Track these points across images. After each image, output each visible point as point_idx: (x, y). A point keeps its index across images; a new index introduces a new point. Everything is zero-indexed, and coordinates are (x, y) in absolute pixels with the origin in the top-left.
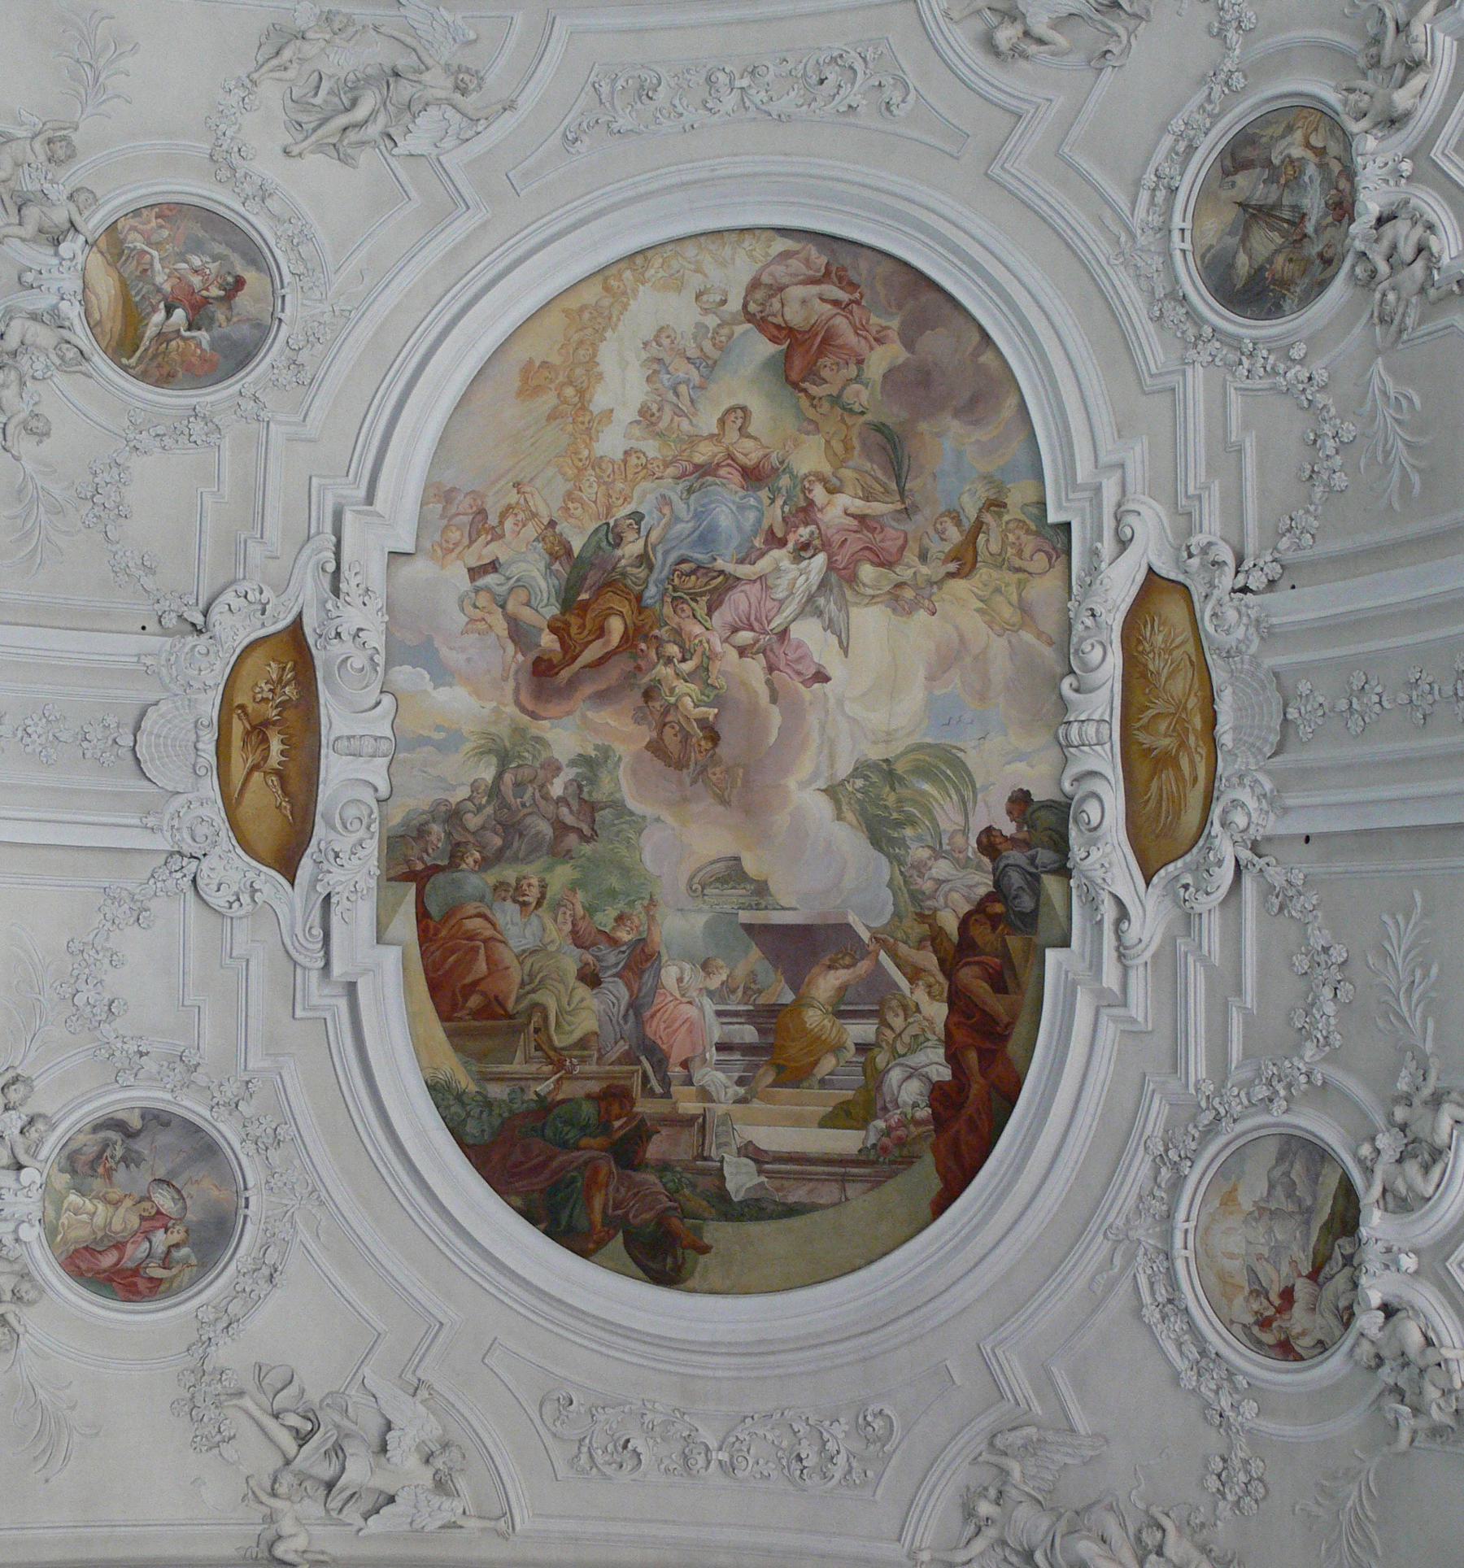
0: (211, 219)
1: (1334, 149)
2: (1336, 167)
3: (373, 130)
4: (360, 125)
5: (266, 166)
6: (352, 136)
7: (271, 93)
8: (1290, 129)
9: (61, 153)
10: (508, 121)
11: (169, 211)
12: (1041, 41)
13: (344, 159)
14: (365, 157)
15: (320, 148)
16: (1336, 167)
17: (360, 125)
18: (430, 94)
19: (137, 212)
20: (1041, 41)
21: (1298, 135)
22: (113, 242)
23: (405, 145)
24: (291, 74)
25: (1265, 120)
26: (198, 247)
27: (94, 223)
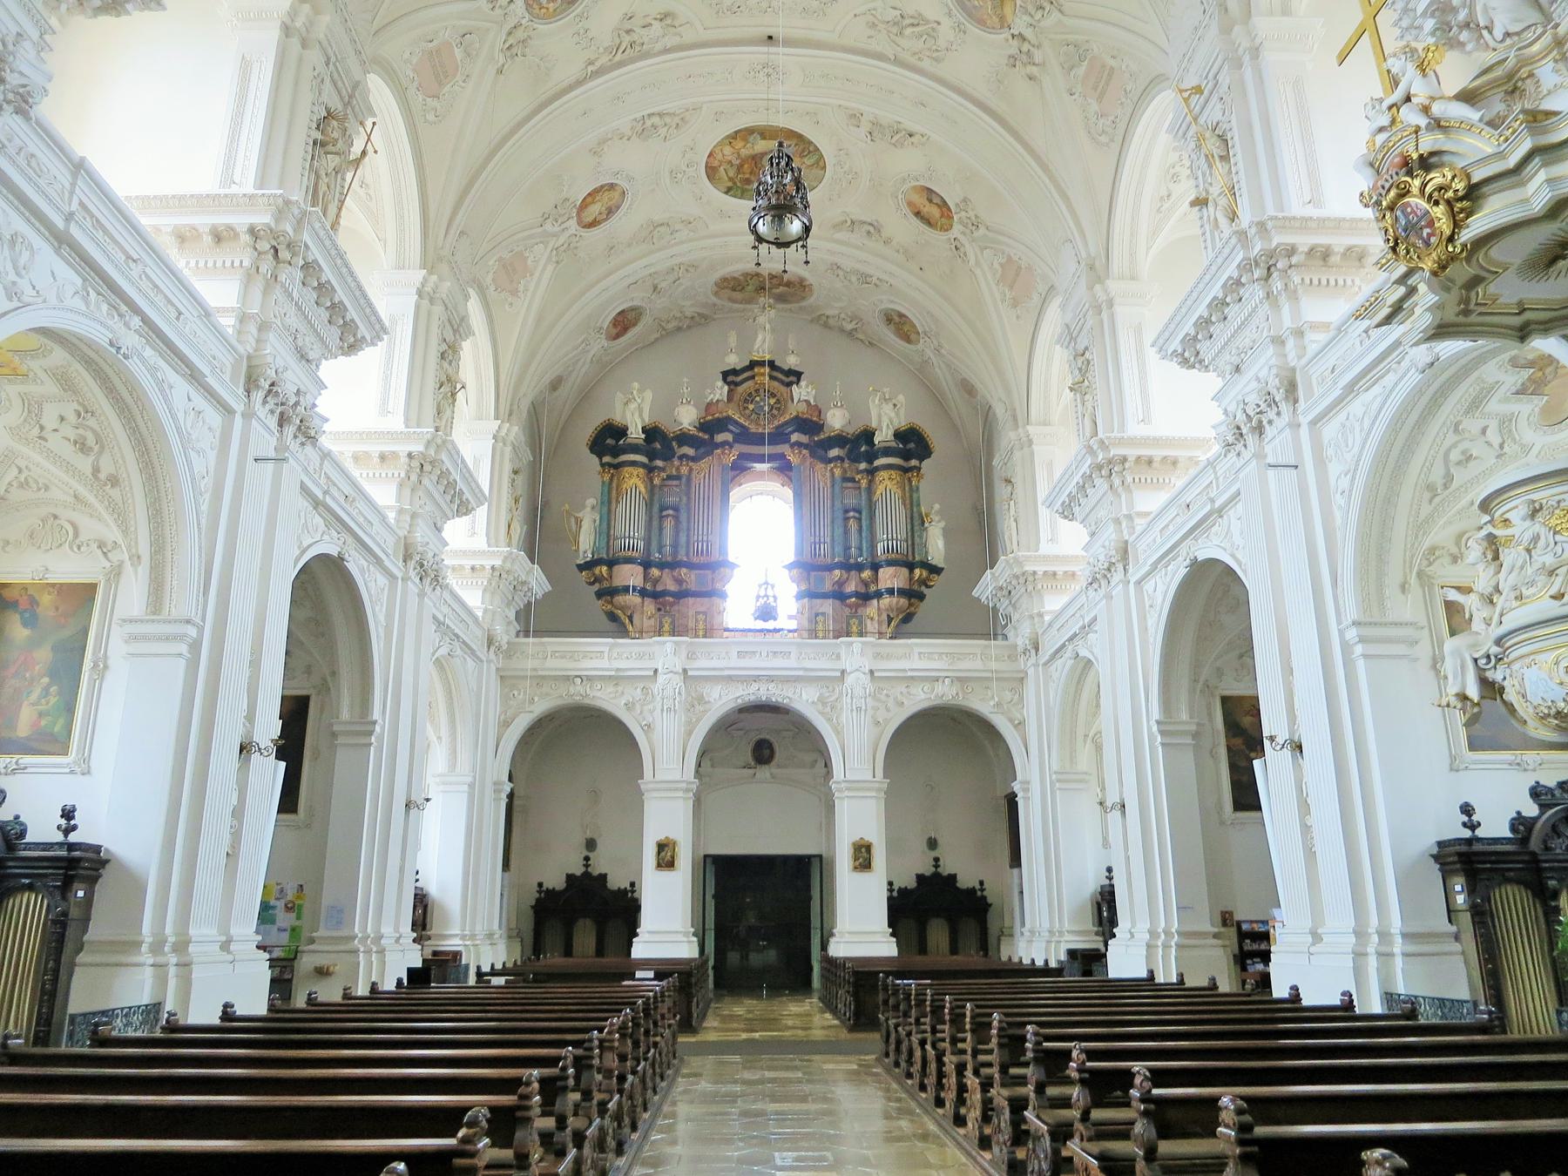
0: (970, 15)
1: (537, 11)
2: (535, 6)
3: (908, 21)
4: (913, 25)
5: (947, 23)
6: (916, 22)
7: (942, 43)
8: (555, 10)
9: (1012, 60)
10: (857, 12)
11: (981, 23)
12: (656, 19)
13: (920, 15)
14: (911, 12)
15: (928, 22)
16: (535, 6)
17: (913, 25)
18: (884, 26)
19: (993, 28)
20: (656, 19)
21: (551, 10)
22: (1003, 23)
23: (898, 12)
24: (935, 47)
25: (565, 10)
26: (975, 7)
27: (1006, 34)
